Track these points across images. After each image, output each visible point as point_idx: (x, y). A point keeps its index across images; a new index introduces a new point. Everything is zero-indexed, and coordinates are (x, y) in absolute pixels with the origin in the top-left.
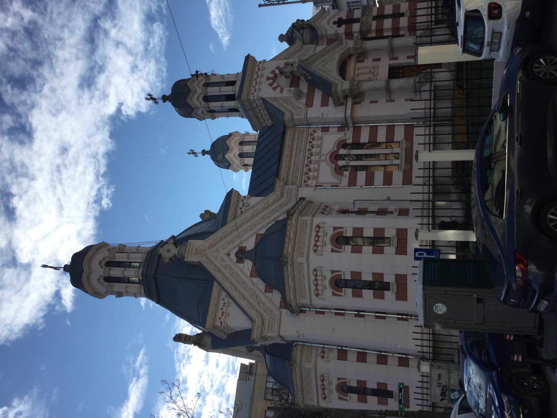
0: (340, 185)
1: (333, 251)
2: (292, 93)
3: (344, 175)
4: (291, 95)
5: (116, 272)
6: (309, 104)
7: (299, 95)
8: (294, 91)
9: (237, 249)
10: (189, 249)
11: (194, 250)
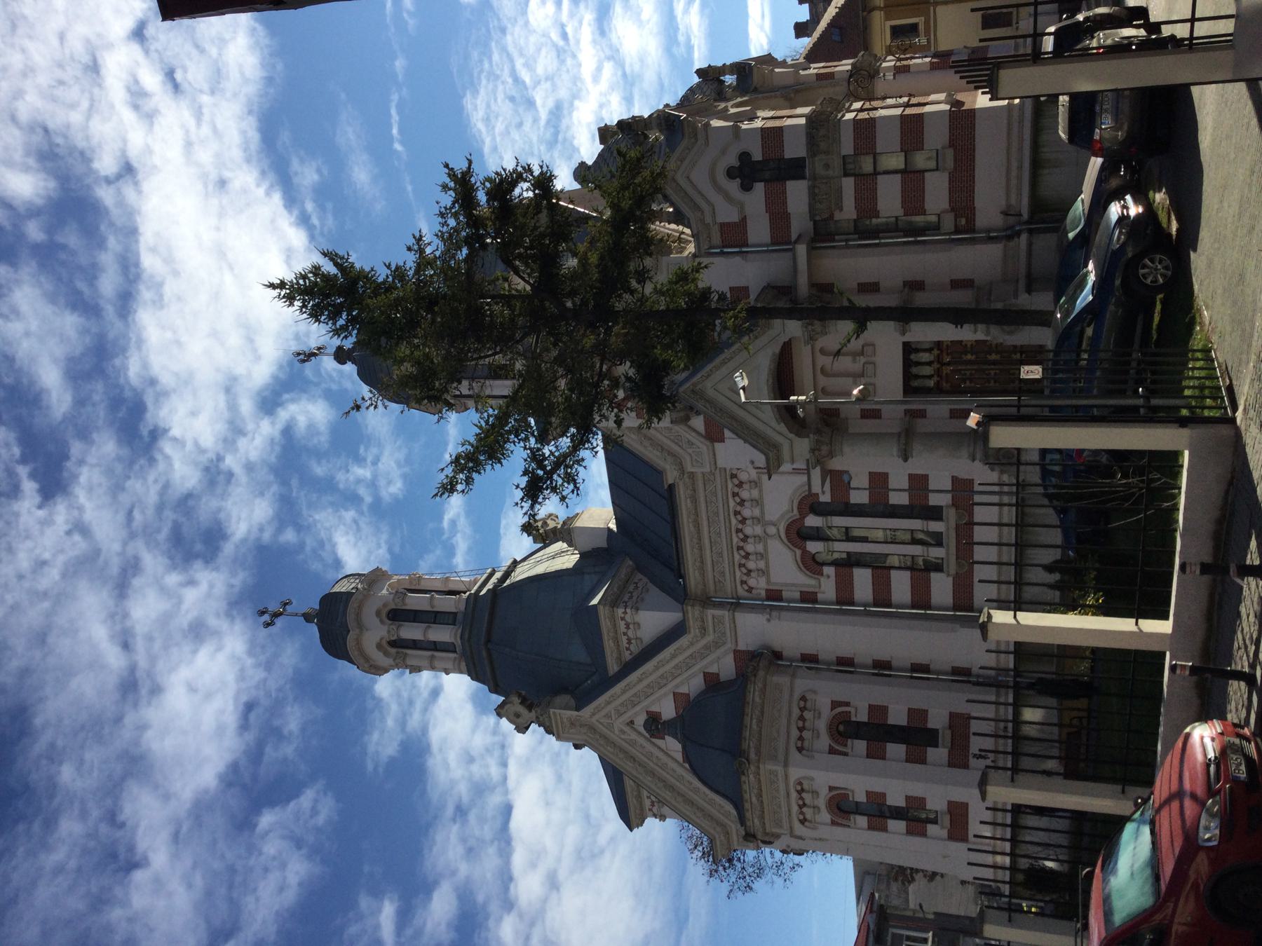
0: (820, 596)
3: (825, 573)
10: (556, 722)
11: (565, 720)
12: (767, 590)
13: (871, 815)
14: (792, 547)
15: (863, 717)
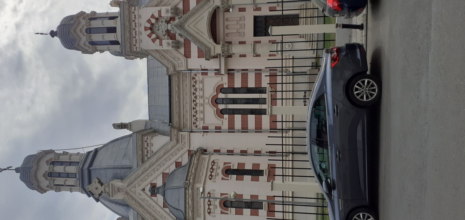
0: (222, 128)
1: (222, 213)
2: (171, 46)
4: (170, 48)
5: (59, 169)
6: (187, 55)
7: (177, 46)
8: (172, 43)
9: (149, 186)
12: (203, 127)
13: (237, 208)
14: (213, 107)
15: (236, 167)
